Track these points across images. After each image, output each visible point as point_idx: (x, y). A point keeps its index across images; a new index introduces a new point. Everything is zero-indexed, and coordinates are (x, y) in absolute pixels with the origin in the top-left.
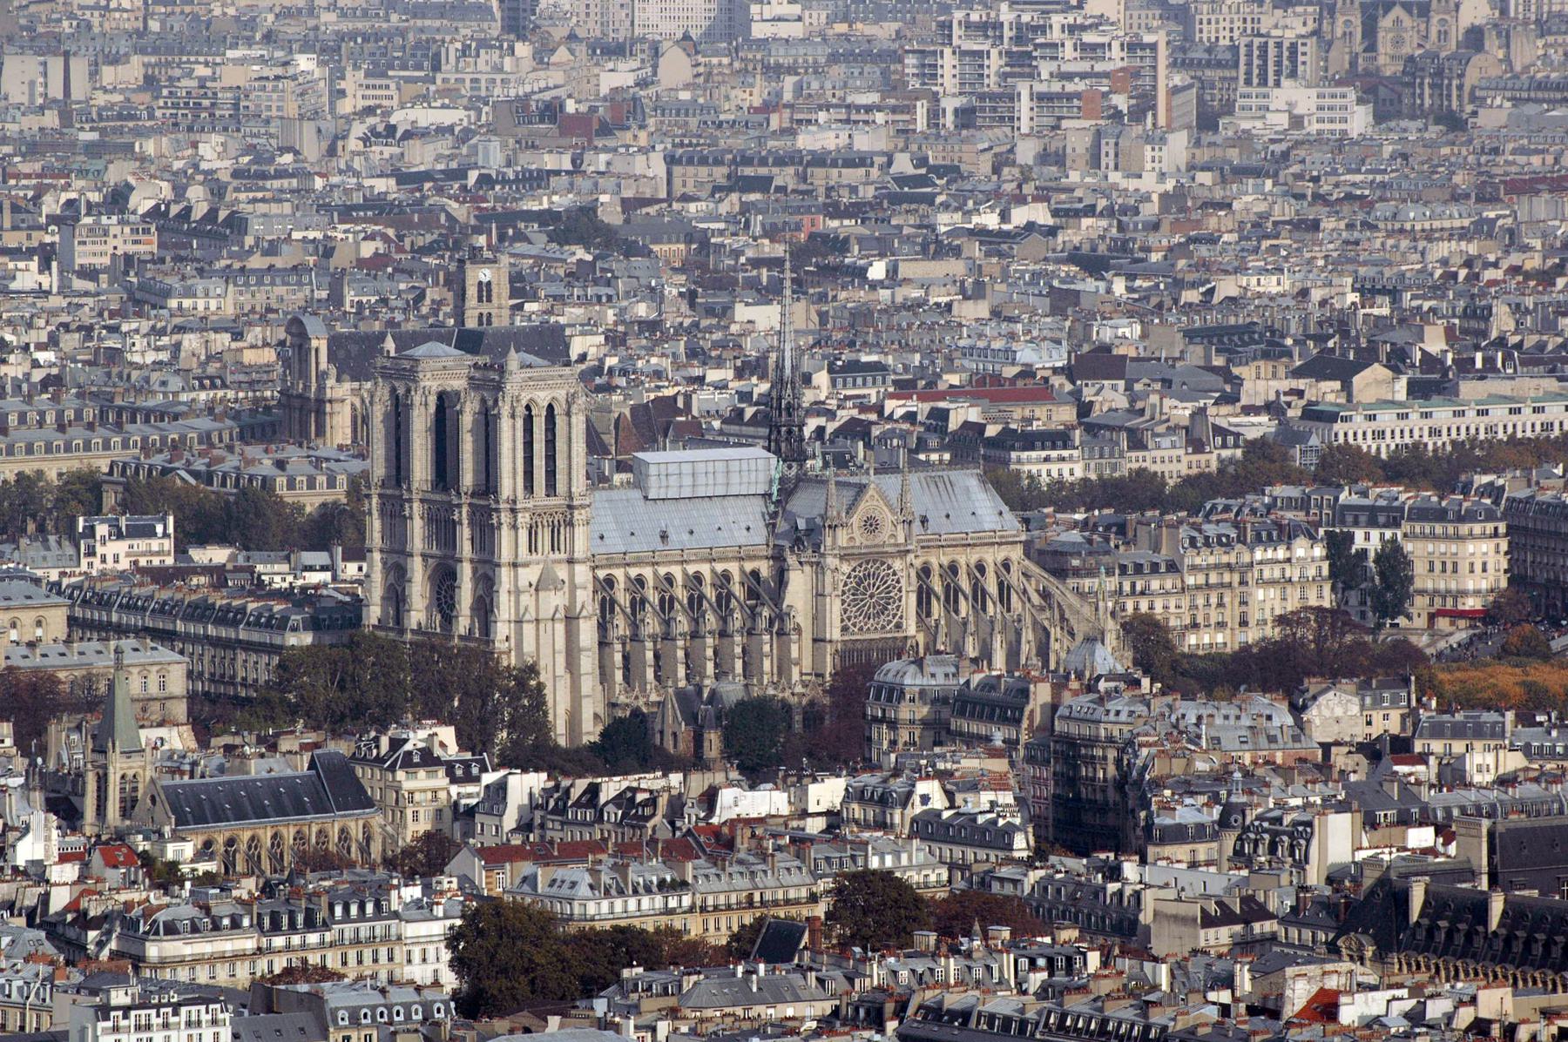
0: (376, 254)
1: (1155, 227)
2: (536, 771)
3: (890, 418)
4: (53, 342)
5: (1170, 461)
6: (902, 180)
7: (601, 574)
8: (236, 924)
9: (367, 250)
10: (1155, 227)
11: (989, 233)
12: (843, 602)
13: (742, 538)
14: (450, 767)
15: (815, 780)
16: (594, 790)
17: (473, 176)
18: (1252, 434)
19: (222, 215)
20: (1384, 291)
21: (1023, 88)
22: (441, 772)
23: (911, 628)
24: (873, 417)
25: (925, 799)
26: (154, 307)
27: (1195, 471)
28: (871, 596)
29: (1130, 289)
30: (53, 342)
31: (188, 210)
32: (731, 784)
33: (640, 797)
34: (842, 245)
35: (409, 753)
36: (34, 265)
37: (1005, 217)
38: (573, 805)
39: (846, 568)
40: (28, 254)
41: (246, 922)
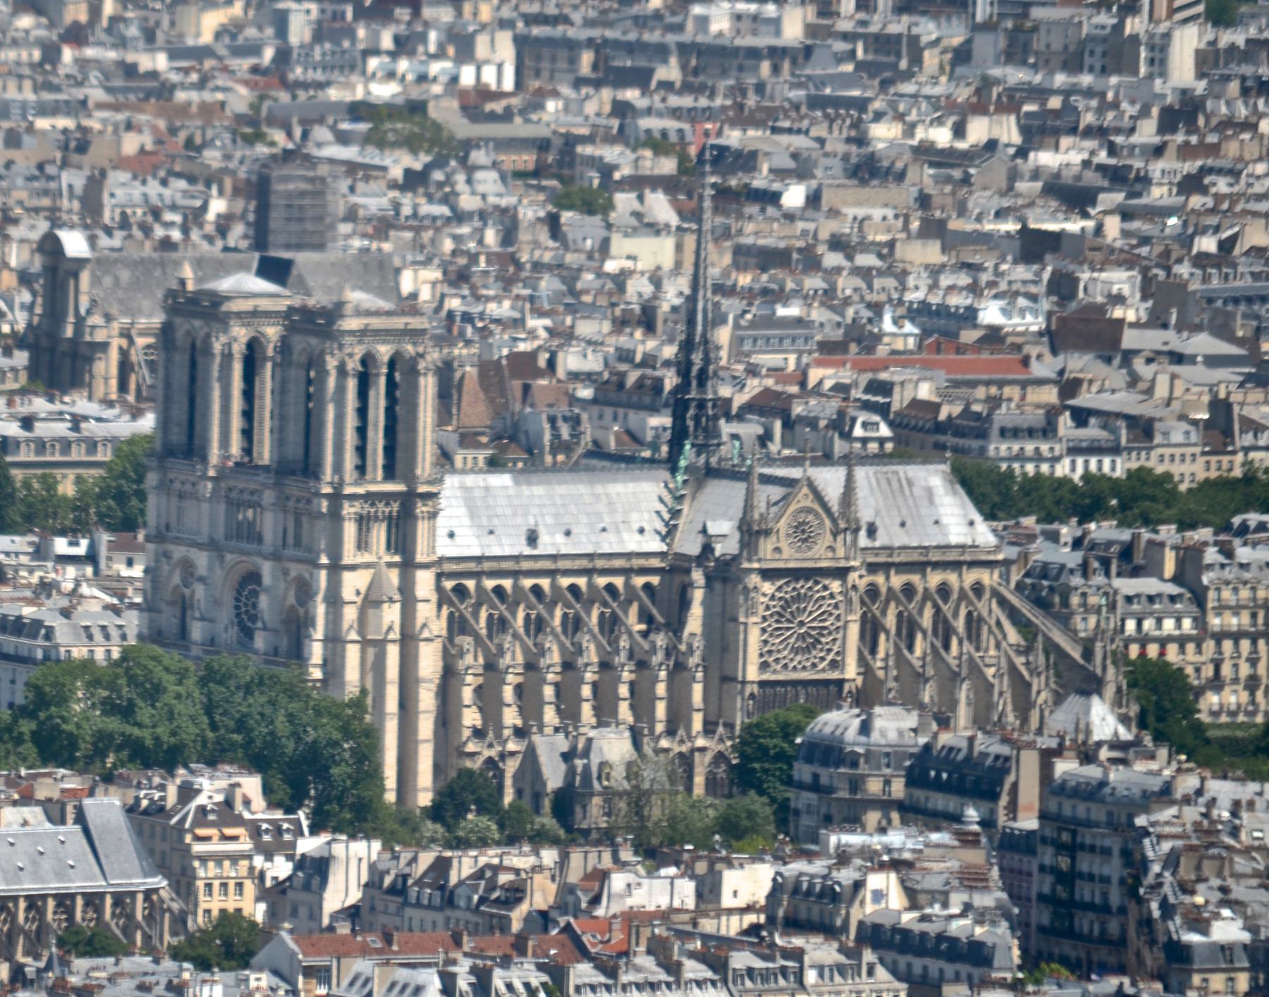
0: (142, 151)
1: (1158, 151)
2: (368, 837)
5: (1184, 462)
7: (449, 584)
9: (131, 144)
10: (1158, 151)
12: (764, 630)
13: (633, 543)
14: (255, 830)
15: (729, 864)
16: (441, 866)
23: (851, 670)
24: (794, 389)
25: (878, 896)
27: (1213, 474)
28: (802, 623)
29: (1125, 234)
32: (621, 865)
33: (504, 878)
34: (747, 160)
35: (202, 810)
37: (959, 131)
38: (415, 884)
39: (768, 588)
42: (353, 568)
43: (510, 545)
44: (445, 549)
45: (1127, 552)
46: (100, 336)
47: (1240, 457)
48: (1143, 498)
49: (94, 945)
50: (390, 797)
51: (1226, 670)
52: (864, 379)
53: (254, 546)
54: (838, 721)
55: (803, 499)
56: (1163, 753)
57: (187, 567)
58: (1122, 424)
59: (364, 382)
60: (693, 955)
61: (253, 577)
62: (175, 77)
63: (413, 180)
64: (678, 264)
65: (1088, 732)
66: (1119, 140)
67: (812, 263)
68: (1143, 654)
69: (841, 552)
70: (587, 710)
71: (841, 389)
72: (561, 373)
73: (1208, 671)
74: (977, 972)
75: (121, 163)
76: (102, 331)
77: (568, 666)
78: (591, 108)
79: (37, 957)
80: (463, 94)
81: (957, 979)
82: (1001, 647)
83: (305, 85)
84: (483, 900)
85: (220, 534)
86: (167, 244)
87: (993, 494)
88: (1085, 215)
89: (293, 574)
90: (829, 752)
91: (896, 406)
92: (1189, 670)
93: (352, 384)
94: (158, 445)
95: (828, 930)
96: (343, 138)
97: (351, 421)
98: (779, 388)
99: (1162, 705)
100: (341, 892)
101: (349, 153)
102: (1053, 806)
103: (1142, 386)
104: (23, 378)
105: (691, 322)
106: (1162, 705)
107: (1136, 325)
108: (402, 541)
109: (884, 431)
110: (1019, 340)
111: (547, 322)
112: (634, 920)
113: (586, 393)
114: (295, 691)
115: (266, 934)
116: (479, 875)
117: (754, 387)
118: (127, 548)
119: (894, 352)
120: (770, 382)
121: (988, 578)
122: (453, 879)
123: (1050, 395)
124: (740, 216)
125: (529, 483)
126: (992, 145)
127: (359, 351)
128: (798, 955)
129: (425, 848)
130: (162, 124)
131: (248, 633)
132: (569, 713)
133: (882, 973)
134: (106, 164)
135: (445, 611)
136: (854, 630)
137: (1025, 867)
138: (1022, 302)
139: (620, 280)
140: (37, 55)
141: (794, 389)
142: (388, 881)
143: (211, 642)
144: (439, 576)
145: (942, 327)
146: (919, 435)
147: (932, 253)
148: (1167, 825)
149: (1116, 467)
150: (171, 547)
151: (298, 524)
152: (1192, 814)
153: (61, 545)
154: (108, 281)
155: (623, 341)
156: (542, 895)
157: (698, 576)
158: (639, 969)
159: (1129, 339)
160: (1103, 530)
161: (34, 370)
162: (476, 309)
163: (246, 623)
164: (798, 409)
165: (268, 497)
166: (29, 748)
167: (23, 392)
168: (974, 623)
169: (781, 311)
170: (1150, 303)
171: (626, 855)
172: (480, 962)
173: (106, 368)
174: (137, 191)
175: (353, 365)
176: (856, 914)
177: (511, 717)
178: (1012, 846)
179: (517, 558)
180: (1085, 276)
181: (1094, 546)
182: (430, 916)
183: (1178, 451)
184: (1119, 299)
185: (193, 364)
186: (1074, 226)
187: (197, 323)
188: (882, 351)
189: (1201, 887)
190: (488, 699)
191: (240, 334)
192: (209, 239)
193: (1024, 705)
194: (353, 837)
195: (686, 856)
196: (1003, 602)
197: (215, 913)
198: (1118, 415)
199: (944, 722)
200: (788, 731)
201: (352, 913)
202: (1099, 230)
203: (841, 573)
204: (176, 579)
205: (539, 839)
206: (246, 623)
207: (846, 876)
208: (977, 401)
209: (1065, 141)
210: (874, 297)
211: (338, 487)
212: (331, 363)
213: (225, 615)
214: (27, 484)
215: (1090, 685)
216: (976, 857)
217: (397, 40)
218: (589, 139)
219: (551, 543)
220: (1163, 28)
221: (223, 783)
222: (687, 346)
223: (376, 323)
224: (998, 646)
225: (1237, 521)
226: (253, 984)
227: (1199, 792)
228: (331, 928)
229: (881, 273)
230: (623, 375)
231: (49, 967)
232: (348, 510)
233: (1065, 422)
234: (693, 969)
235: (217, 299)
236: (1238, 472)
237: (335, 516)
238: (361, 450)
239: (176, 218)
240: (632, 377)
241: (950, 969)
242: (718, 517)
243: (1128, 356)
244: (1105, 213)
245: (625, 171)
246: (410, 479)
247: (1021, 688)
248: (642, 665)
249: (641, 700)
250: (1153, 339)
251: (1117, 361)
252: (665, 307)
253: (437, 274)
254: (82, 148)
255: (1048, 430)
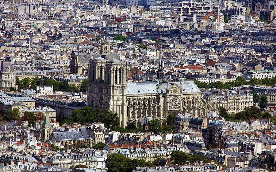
1: (219, 39)
3: (175, 72)
4: (30, 55)
5: (224, 80)
6: (174, 30)
7: (128, 98)
8: (68, 157)
9: (83, 40)
11: (190, 40)
13: (152, 92)
14: (103, 131)
15: (167, 135)
16: (128, 135)
17: (100, 28)
18: (238, 76)
19: (58, 34)
20: (259, 51)
21: (195, 15)
22: (102, 132)
23: (181, 108)
24: (172, 71)
25: (186, 138)
26: (47, 50)
27: (228, 82)
28: (175, 102)
29: (215, 50)
30: (30, 55)
31: (52, 33)
33: (136, 137)
36: (26, 42)
37: (193, 37)
39: (170, 98)
40: (25, 40)
41: (70, 157)
42: (115, 96)
43: (136, 92)
44: (128, 93)
45: (217, 92)
46: (80, 66)
47: (231, 79)
48: (218, 85)
49: (82, 147)
50: (121, 126)
51: (231, 108)
52: (182, 70)
53: (102, 94)
54: (180, 115)
55: (175, 86)
56: (223, 119)
57: (93, 96)
58: (216, 75)
59: (116, 71)
60: (162, 146)
61: (102, 97)
62: (88, 31)
63: (121, 45)
64: (156, 55)
65: (213, 116)
66: (214, 38)
67: (174, 54)
68: (220, 106)
69: (180, 93)
70: (146, 114)
71: (179, 71)
72: (141, 70)
73: (228, 108)
74: (200, 148)
75: (82, 43)
76: (80, 65)
77: (144, 109)
78: (144, 35)
79: (75, 148)
80: (126, 33)
81: (197, 149)
82: (201, 105)
83: (106, 32)
84: (134, 140)
85: (97, 92)
86: (88, 53)
87: (200, 85)
88: (210, 48)
89: (107, 97)
90: (179, 119)
91: (186, 73)
92: (226, 108)
93: (115, 71)
94: (89, 80)
95: (180, 143)
96: (111, 39)
97: (115, 77)
98: (170, 71)
99: (223, 112)
100: (115, 139)
101: (112, 41)
102: (209, 126)
103: (218, 70)
104: (70, 72)
105: (160, 62)
106: (223, 112)
107: (217, 62)
108: (122, 93)
109: (184, 77)
110: (202, 64)
111: (139, 63)
112: (153, 142)
113: (145, 72)
114: (109, 113)
115: (105, 145)
116: (133, 136)
117: (167, 71)
118: (85, 94)
119: (185, 66)
120: (169, 70)
121: (200, 96)
122: (130, 137)
123: (206, 72)
124: (164, 48)
125: (138, 84)
126: (197, 39)
127: (116, 67)
128: (176, 146)
129: (126, 133)
130: (87, 38)
131: (101, 105)
132: (144, 115)
133: (187, 149)
134: (80, 43)
135: (127, 102)
136: (182, 103)
137: (205, 134)
138: (202, 59)
139: (149, 57)
140: (70, 29)
141: (172, 71)
142: (121, 137)
143: (96, 107)
144: (127, 97)
145: (191, 63)
146: (189, 77)
147: (190, 53)
148: (225, 128)
149: (215, 81)
150: (91, 94)
151: (108, 90)
152: (227, 127)
153: (76, 94)
154: (81, 58)
155: (149, 65)
156: (142, 139)
157: (161, 96)
158: (155, 149)
159: (216, 64)
160: (214, 89)
161: (71, 70)
162: (130, 61)
163: (101, 103)
164: (173, 74)
165: (104, 87)
166: (72, 121)
167: (70, 73)
168: (198, 102)
169: (170, 61)
170: (219, 59)
171: (153, 133)
172: (134, 148)
173: (81, 70)
174: (84, 47)
175: (115, 69)
176: (184, 141)
177: (136, 115)
178: (204, 131)
179: (137, 94)
180: (210, 56)
181: (213, 91)
182: (127, 142)
183: (223, 79)
184: (215, 59)
185: (93, 69)
186: (208, 49)
187: (94, 64)
188: (184, 66)
189: (229, 136)
190: (133, 113)
191: (100, 65)
192: (94, 53)
193: (204, 113)
194: (116, 132)
195: (161, 133)
196: (201, 99)
197: (98, 142)
198: (215, 74)
199: (194, 115)
200: (174, 117)
201: (116, 142)
202: (212, 50)
203: (180, 95)
204: (92, 98)
205: (141, 132)
206: (101, 103)
207: (182, 136)
208: (197, 73)
209: (207, 38)
210: (182, 59)
211: (113, 85)
212: (112, 69)
213: (98, 103)
214: (71, 85)
215: (213, 110)
216: (199, 133)
217: (117, 26)
218: (143, 39)
219: (141, 92)
220: (219, 23)
221: (99, 125)
222: (159, 66)
223: (118, 63)
224: (201, 105)
225: (231, 88)
226: (104, 152)
227: (228, 124)
228: (114, 144)
229: (183, 56)
230: (150, 70)
231: (76, 150)
232: (115, 88)
233: (208, 75)
234: (162, 148)
235: (96, 61)
236: (231, 81)
237: (113, 89)
238: (116, 80)
239: (90, 50)
240: (151, 70)
241: (196, 148)
242: (164, 87)
243: (216, 66)
244: (212, 47)
245: (149, 43)
246: (123, 84)
247: (204, 110)
248: (154, 108)
249: (154, 114)
250: (220, 64)
251: (215, 67)
252: (155, 61)
253: (124, 57)
254: (76, 41)
255: (206, 76)
